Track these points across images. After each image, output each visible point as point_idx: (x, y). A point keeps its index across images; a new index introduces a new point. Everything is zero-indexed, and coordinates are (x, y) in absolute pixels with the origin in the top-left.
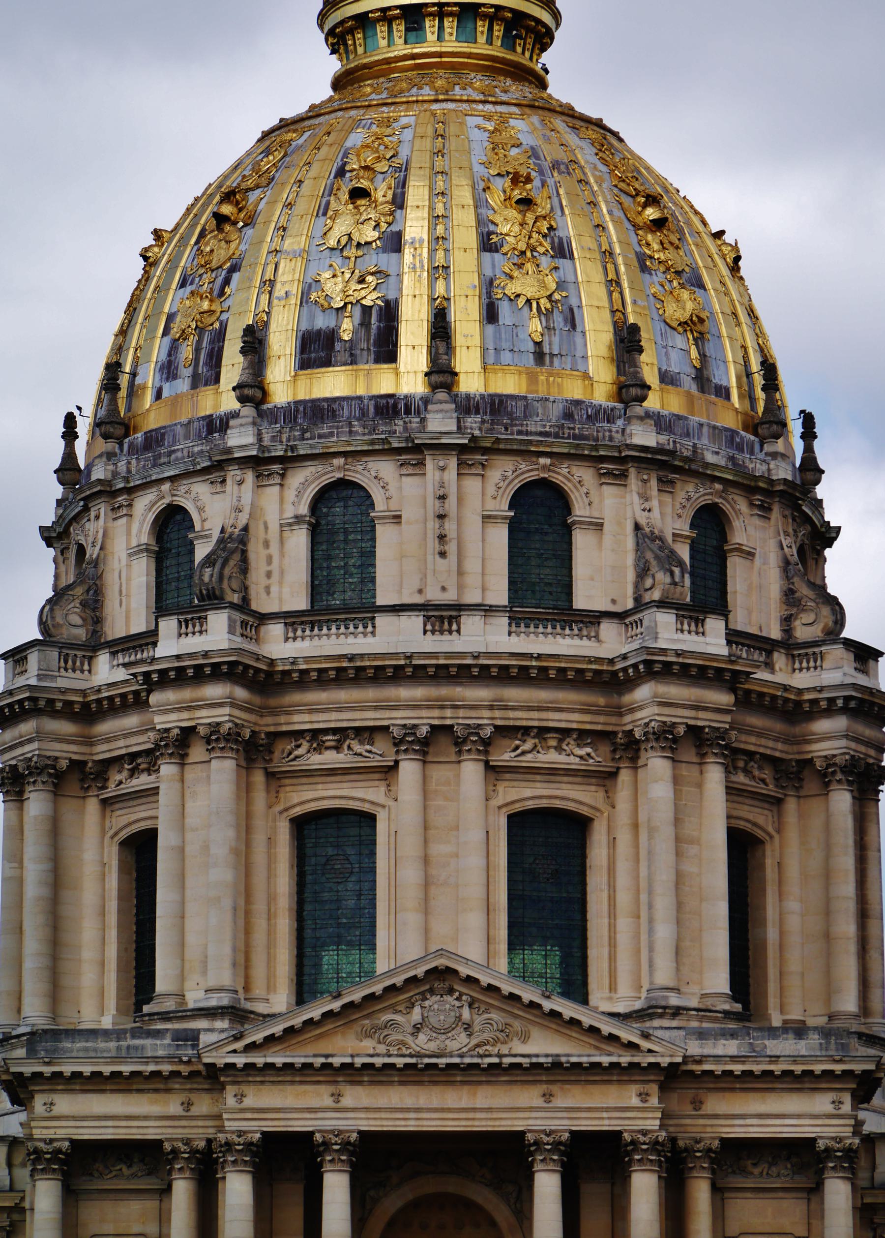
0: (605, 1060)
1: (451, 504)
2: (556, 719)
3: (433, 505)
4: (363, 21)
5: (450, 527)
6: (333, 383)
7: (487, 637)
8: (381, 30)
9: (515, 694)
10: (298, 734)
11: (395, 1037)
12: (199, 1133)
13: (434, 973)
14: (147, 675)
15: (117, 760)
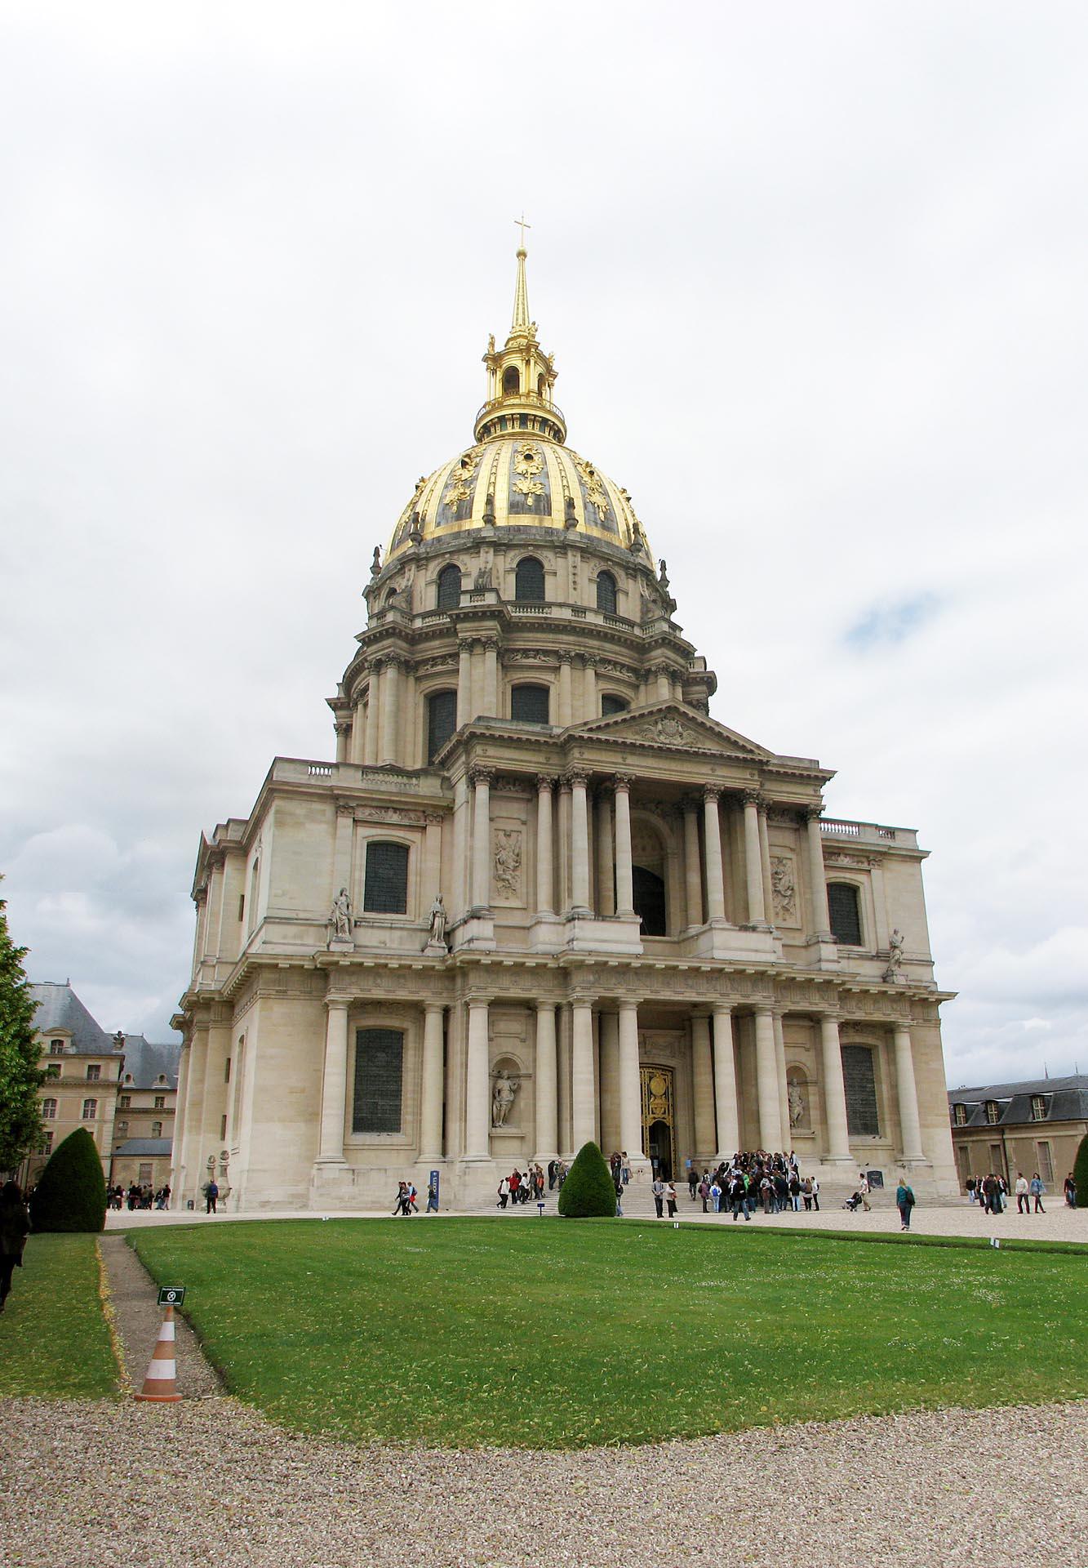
0: (741, 755)
1: (578, 571)
2: (621, 659)
3: (571, 570)
4: (502, 419)
5: (578, 579)
6: (525, 520)
7: (595, 620)
8: (510, 424)
9: (608, 646)
10: (518, 650)
11: (650, 735)
12: (555, 772)
13: (669, 708)
14: (458, 615)
15: (425, 662)
